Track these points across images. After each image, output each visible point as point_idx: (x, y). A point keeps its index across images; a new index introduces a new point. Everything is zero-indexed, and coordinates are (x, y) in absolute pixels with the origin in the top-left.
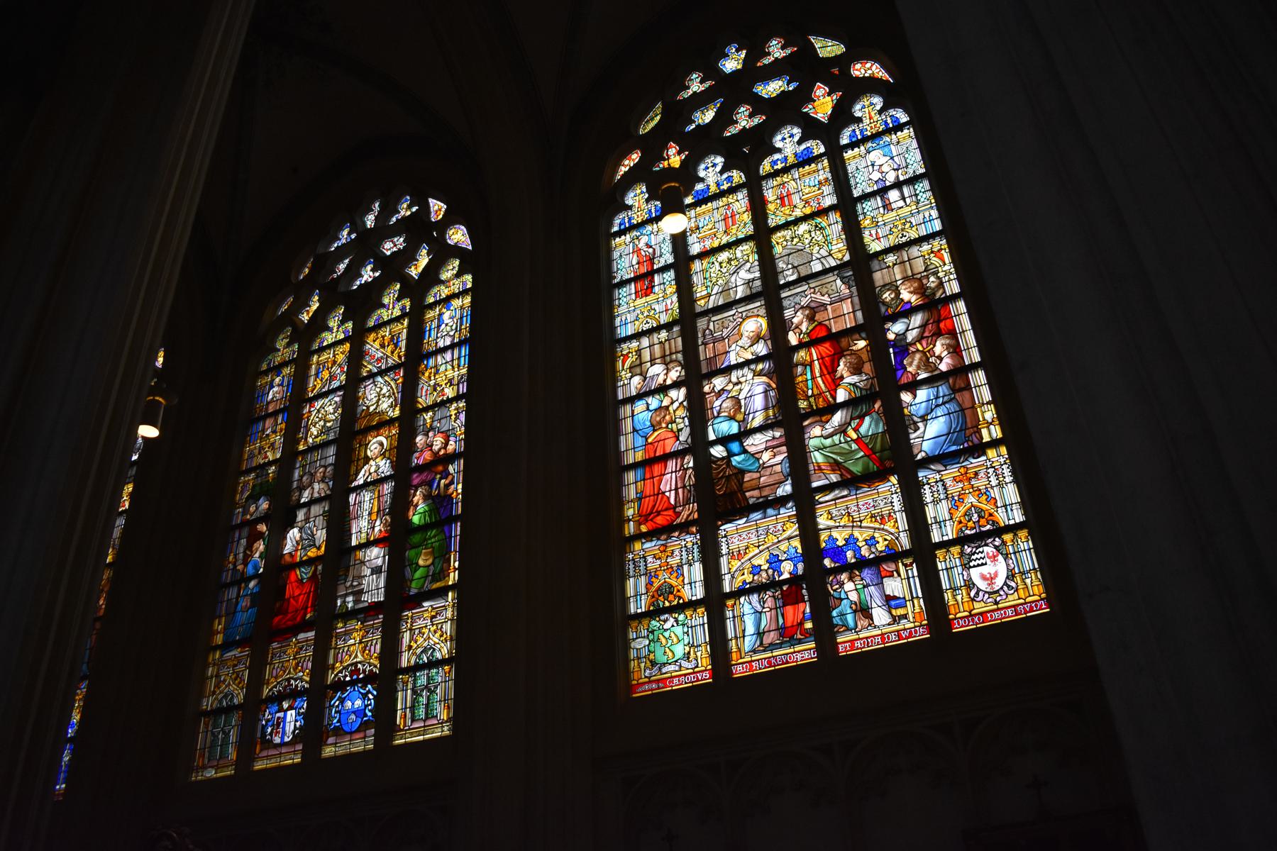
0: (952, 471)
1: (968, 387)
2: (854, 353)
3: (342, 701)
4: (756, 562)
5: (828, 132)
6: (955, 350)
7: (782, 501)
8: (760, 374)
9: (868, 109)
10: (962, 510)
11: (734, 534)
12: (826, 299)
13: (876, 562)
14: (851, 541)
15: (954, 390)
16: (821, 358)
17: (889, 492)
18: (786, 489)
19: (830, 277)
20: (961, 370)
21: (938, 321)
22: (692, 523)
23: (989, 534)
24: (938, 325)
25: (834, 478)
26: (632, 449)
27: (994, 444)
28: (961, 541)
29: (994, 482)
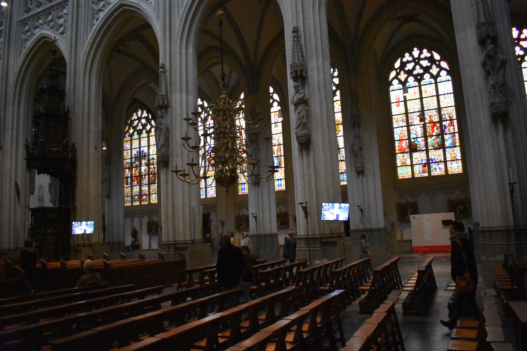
0: (451, 149)
1: (455, 136)
3: (343, 176)
5: (435, 77)
6: (454, 129)
7: (423, 150)
8: (420, 127)
9: (443, 73)
10: (451, 156)
11: (415, 155)
12: (433, 115)
13: (438, 162)
14: (434, 159)
15: (453, 136)
16: (431, 126)
17: (441, 151)
18: (424, 148)
19: (434, 110)
20: (454, 133)
21: (452, 123)
22: (408, 152)
23: (455, 160)
24: (452, 124)
25: (432, 148)
26: (397, 137)
27: (458, 146)
28: (451, 161)
29: (457, 152)
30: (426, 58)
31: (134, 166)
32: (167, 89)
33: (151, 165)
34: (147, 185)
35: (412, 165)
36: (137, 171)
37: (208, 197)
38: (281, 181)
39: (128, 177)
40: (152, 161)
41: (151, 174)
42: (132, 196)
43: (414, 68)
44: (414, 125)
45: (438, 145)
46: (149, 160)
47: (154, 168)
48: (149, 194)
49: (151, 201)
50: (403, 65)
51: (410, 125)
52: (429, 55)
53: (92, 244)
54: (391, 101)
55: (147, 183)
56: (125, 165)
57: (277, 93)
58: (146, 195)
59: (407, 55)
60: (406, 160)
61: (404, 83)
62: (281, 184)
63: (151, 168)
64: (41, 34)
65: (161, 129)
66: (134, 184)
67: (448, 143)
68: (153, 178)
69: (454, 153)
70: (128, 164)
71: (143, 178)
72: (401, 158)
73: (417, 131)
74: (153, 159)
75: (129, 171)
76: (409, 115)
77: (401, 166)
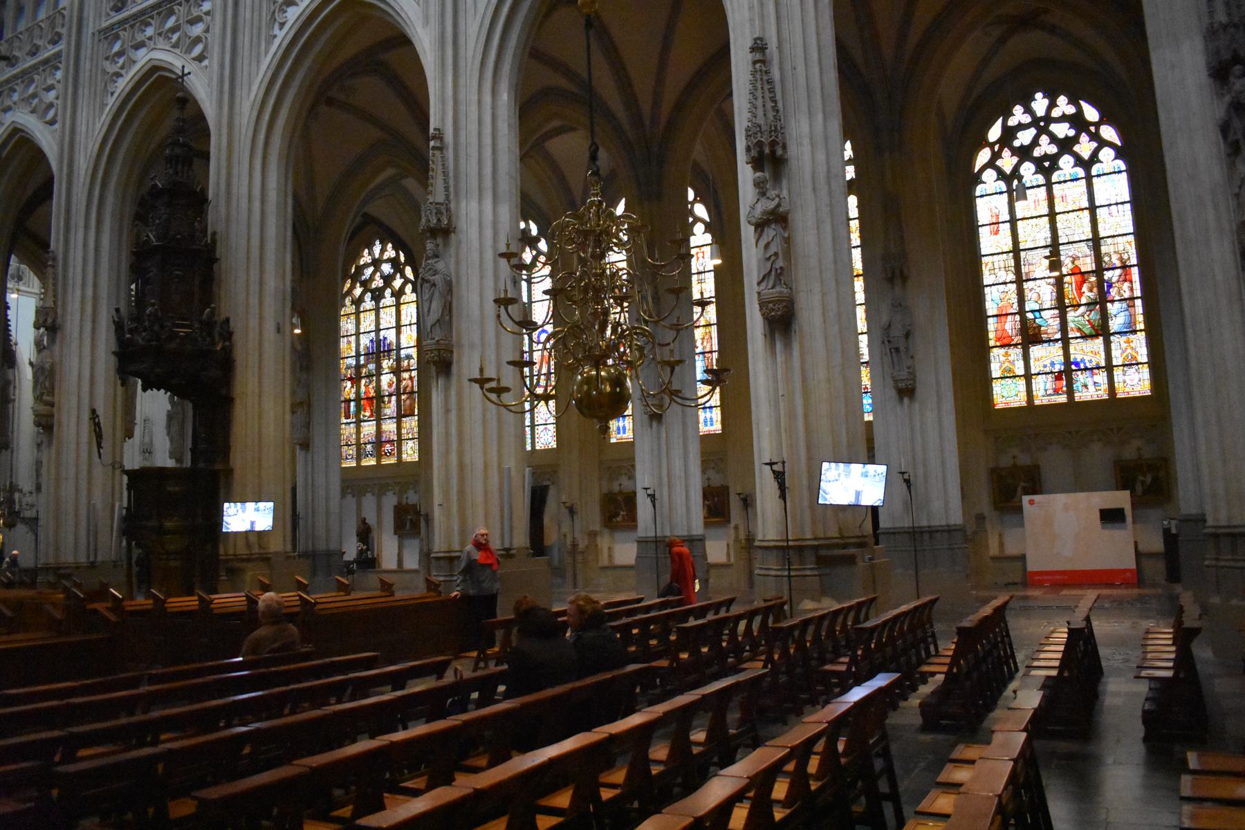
0: (1124, 338)
1: (1134, 306)
2: (1090, 282)
4: (1045, 363)
5: (1086, 165)
6: (1132, 289)
7: (1057, 340)
9: (1107, 154)
10: (1125, 354)
11: (1035, 351)
12: (1080, 255)
13: (1092, 369)
14: (1083, 360)
15: (1129, 306)
16: (1076, 282)
17: (1099, 342)
18: (1058, 336)
19: (1083, 244)
20: (1132, 299)
21: (1126, 275)
22: (1019, 344)
23: (1134, 364)
24: (1126, 278)
25: (1078, 334)
26: (991, 308)
27: (1141, 331)
28: (1124, 365)
30: (1064, 118)
31: (363, 375)
32: (447, 189)
33: (404, 371)
34: (393, 418)
35: (1028, 377)
36: (371, 386)
37: (537, 448)
38: (711, 412)
39: (350, 401)
40: (406, 361)
41: (404, 394)
42: (358, 445)
43: (1035, 142)
44: (1035, 279)
45: (1093, 327)
46: (398, 360)
47: (411, 378)
48: (400, 440)
49: (404, 456)
50: (1009, 134)
51: (1024, 278)
52: (1071, 110)
53: (269, 556)
54: (978, 221)
55: (395, 415)
56: (343, 371)
57: (703, 201)
58: (390, 442)
59: (1018, 110)
60: (1013, 363)
61: (1008, 178)
62: (711, 419)
63: (405, 380)
64: (151, 59)
65: (434, 285)
66: (364, 416)
67: (1115, 324)
68: (408, 402)
69: (1132, 348)
70: (349, 368)
71: (384, 402)
72: (1002, 359)
73: (1041, 293)
74: (409, 357)
75: (352, 387)
76: (1023, 254)
77: (1001, 378)
